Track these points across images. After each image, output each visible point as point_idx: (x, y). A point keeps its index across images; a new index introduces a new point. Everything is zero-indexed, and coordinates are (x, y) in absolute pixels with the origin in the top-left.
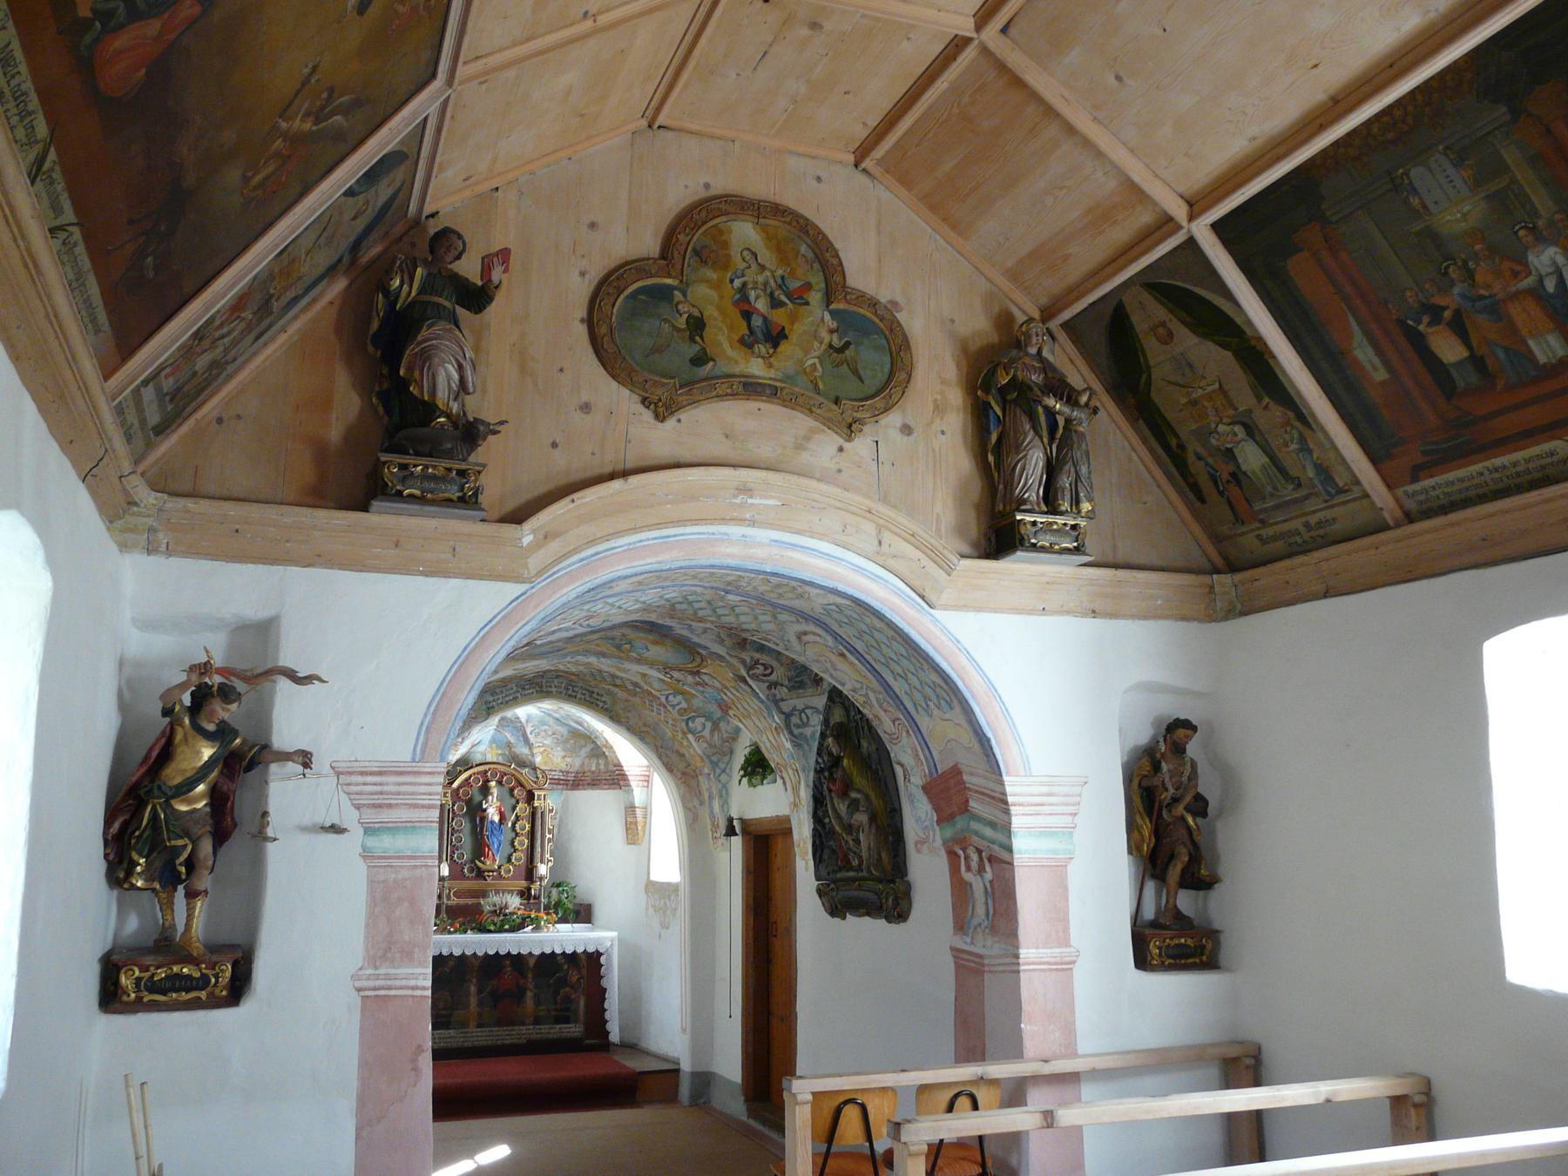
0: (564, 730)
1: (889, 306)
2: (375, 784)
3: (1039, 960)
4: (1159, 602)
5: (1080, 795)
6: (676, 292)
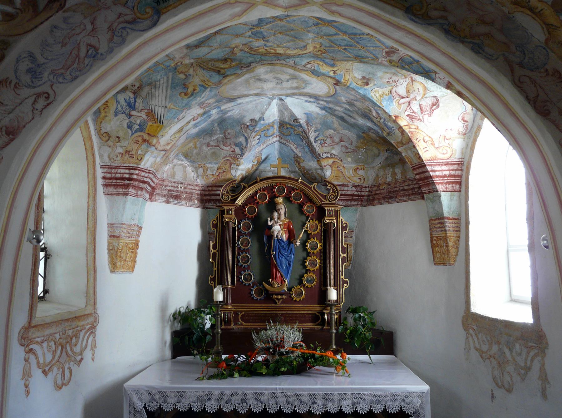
0: (351, 135)
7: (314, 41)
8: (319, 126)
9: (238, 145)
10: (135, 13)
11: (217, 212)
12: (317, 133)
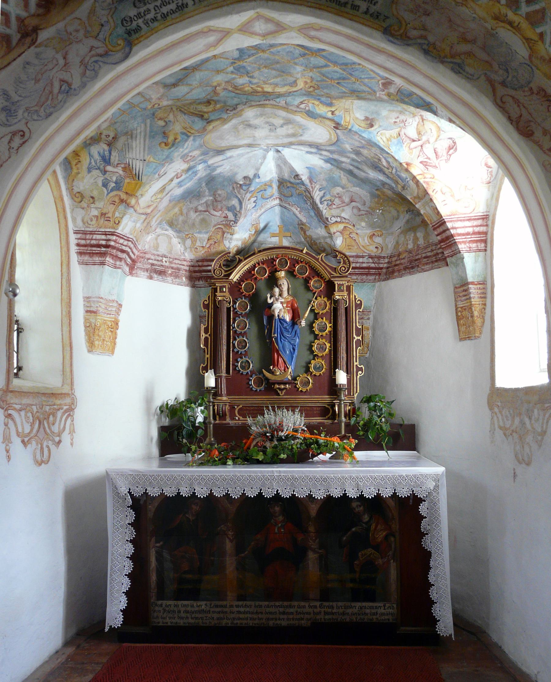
0: (362, 192)
7: (303, 76)
8: (324, 183)
9: (231, 209)
10: (106, 45)
11: (208, 291)
12: (323, 192)
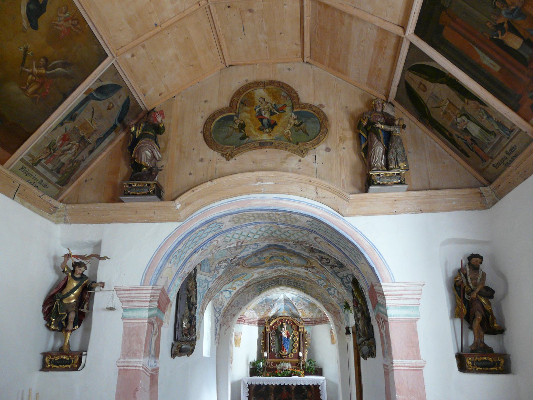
1: (319, 107)
2: (128, 294)
3: (404, 365)
4: (454, 203)
5: (421, 290)
6: (235, 117)
9: (271, 306)
11: (264, 328)
